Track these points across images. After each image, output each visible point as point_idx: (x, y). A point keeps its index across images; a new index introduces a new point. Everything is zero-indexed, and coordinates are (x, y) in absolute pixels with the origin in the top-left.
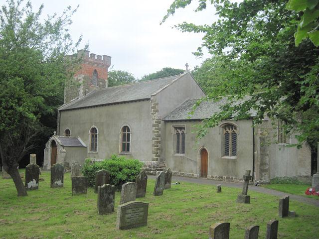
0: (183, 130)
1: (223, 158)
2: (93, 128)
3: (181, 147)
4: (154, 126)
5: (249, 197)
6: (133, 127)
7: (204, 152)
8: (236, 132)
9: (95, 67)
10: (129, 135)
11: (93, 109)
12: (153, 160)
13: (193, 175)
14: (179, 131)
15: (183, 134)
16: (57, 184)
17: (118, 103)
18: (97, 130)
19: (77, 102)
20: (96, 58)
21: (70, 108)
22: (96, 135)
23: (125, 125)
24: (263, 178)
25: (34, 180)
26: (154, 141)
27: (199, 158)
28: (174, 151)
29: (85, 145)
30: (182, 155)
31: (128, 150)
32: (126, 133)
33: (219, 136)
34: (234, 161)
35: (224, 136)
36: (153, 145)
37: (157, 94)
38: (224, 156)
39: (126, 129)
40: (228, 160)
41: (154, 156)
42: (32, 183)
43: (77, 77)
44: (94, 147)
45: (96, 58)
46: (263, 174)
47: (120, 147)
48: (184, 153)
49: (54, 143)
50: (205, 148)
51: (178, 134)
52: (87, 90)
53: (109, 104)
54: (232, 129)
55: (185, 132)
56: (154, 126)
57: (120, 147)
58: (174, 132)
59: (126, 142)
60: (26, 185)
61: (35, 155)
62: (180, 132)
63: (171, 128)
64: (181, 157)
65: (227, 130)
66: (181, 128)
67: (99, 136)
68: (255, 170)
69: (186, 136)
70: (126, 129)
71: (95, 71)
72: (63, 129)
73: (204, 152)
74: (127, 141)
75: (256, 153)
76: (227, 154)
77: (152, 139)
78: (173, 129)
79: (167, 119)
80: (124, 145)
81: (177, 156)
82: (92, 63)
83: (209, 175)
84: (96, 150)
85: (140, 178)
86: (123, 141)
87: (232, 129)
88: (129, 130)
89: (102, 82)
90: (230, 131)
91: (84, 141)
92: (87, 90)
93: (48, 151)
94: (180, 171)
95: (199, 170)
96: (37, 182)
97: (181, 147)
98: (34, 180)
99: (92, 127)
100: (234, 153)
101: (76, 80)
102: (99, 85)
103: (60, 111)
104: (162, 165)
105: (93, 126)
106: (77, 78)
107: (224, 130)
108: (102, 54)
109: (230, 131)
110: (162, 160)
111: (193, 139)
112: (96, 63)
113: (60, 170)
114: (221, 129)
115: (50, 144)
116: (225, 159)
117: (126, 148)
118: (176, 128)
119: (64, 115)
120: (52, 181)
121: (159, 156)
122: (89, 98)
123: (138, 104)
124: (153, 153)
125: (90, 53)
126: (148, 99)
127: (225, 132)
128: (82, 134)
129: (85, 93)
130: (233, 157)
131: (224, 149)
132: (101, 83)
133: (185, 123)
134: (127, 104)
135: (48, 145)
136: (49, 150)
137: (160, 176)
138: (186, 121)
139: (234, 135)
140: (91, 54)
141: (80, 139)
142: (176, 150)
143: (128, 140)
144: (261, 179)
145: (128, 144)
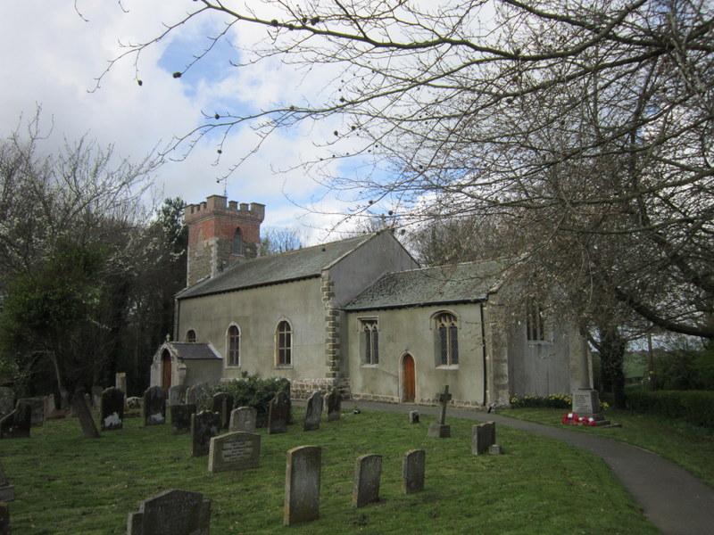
0: (375, 325)
1: (439, 368)
3: (372, 355)
4: (327, 319)
5: (448, 427)
6: (298, 324)
7: (408, 360)
9: (237, 223)
10: (289, 335)
11: (232, 295)
12: (328, 376)
13: (392, 399)
14: (369, 326)
15: (375, 331)
16: (155, 420)
17: (271, 284)
19: (207, 284)
20: (239, 208)
21: (195, 294)
22: (238, 339)
23: (282, 320)
24: (500, 399)
25: (115, 413)
26: (328, 344)
27: (400, 371)
28: (362, 360)
29: (219, 356)
30: (374, 366)
31: (289, 361)
32: (285, 332)
33: (431, 333)
34: (455, 373)
35: (439, 332)
36: (327, 352)
37: (331, 267)
38: (437, 365)
39: (284, 326)
40: (446, 372)
41: (328, 369)
42: (113, 419)
43: (205, 241)
44: (233, 358)
45: (239, 208)
46: (500, 392)
47: (275, 356)
48: (377, 362)
49: (166, 354)
50: (409, 352)
51: (367, 331)
52: (224, 263)
53: (256, 286)
54: (450, 320)
55: (377, 326)
56: (327, 319)
57: (275, 356)
58: (360, 328)
59: (285, 348)
60: (103, 422)
61: (124, 375)
64: (373, 369)
65: (443, 322)
66: (372, 322)
69: (380, 334)
70: (284, 326)
72: (184, 330)
73: (408, 360)
74: (283, 350)
75: (487, 358)
76: (445, 362)
78: (360, 323)
79: (349, 308)
80: (281, 353)
81: (366, 369)
82: (232, 217)
83: (417, 400)
84: (237, 363)
85: (276, 402)
86: (281, 346)
88: (289, 329)
89: (250, 248)
90: (447, 324)
91: (218, 348)
92: (224, 263)
93: (156, 367)
94: (372, 393)
95: (401, 391)
96: (121, 417)
97: (372, 355)
98: (115, 413)
100: (455, 361)
101: (205, 245)
102: (246, 253)
103: (179, 299)
104: (343, 384)
105: (232, 324)
107: (438, 322)
108: (248, 201)
109: (447, 324)
110: (342, 376)
111: (391, 339)
112: (239, 217)
113: (159, 396)
114: (433, 321)
115: (160, 356)
117: (285, 357)
118: (364, 322)
119: (185, 305)
120: (147, 414)
121: (338, 370)
122: (228, 275)
123: (302, 282)
124: (328, 364)
125: (228, 200)
126: (317, 276)
127: (439, 325)
128: (215, 336)
129: (221, 268)
130: (454, 367)
131: (440, 355)
132: (248, 250)
133: (376, 312)
134: (290, 284)
135: (157, 359)
136: (159, 366)
137: (311, 400)
138: (378, 309)
139: (454, 330)
140: (230, 202)
141: (211, 346)
142: (364, 358)
143: (289, 345)
144: (497, 401)
145: (289, 351)
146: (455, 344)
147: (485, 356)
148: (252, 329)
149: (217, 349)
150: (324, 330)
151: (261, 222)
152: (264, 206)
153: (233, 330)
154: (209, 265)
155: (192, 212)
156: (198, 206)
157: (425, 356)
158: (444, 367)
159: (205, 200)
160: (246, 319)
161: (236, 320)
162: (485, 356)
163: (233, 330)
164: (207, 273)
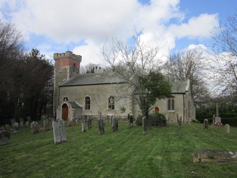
2: (87, 97)
8: (174, 99)
18: (91, 98)
34: (174, 113)
40: (171, 113)
50: (158, 107)
54: (172, 98)
67: (92, 102)
68: (185, 116)
71: (75, 64)
75: (185, 109)
76: (170, 110)
77: (129, 102)
84: (89, 108)
87: (172, 98)
99: (86, 96)
100: (173, 109)
101: (64, 68)
105: (88, 96)
106: (65, 68)
112: (75, 60)
116: (169, 112)
124: (130, 109)
129: (70, 76)
131: (168, 107)
139: (173, 101)
141: (77, 103)
146: (173, 105)
147: (184, 108)
149: (80, 104)
151: (80, 62)
152: (81, 56)
153: (88, 98)
154: (66, 75)
155: (58, 56)
156: (61, 54)
159: (65, 53)
160: (94, 95)
161: (89, 94)
162: (184, 108)
163: (88, 98)
164: (65, 78)
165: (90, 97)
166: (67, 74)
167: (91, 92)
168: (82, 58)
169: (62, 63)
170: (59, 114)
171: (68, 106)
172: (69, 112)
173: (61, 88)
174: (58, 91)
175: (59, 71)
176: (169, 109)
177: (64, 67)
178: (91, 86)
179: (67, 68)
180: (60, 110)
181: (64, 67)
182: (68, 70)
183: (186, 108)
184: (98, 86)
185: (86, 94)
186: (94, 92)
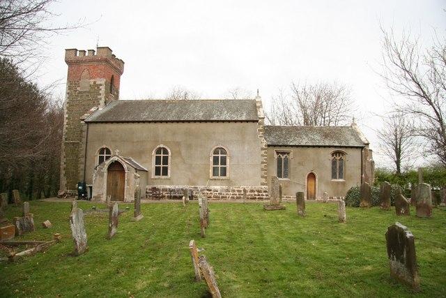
7: (312, 176)
15: (286, 160)
18: (169, 151)
34: (343, 184)
40: (338, 183)
51: (279, 161)
56: (262, 149)
58: (276, 156)
62: (283, 157)
63: (274, 150)
66: (283, 153)
101: (92, 83)
105: (162, 146)
106: (95, 83)
118: (278, 153)
124: (262, 177)
138: (292, 146)
145: (225, 169)
148: (183, 152)
150: (260, 156)
154: (98, 100)
157: (325, 172)
158: (335, 180)
160: (178, 144)
165: (166, 148)
166: (99, 97)
167: (169, 139)
168: (127, 69)
169: (86, 71)
170: (100, 185)
171: (125, 166)
172: (128, 180)
173: (92, 127)
174: (85, 134)
175: (78, 89)
176: (334, 176)
177: (92, 82)
178: (169, 125)
179: (98, 83)
180: (102, 175)
181: (92, 82)
182: (103, 89)
183: (366, 175)
184: (186, 125)
185: (157, 142)
186: (179, 139)
